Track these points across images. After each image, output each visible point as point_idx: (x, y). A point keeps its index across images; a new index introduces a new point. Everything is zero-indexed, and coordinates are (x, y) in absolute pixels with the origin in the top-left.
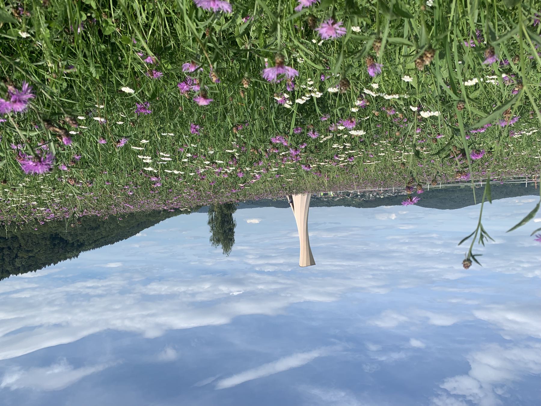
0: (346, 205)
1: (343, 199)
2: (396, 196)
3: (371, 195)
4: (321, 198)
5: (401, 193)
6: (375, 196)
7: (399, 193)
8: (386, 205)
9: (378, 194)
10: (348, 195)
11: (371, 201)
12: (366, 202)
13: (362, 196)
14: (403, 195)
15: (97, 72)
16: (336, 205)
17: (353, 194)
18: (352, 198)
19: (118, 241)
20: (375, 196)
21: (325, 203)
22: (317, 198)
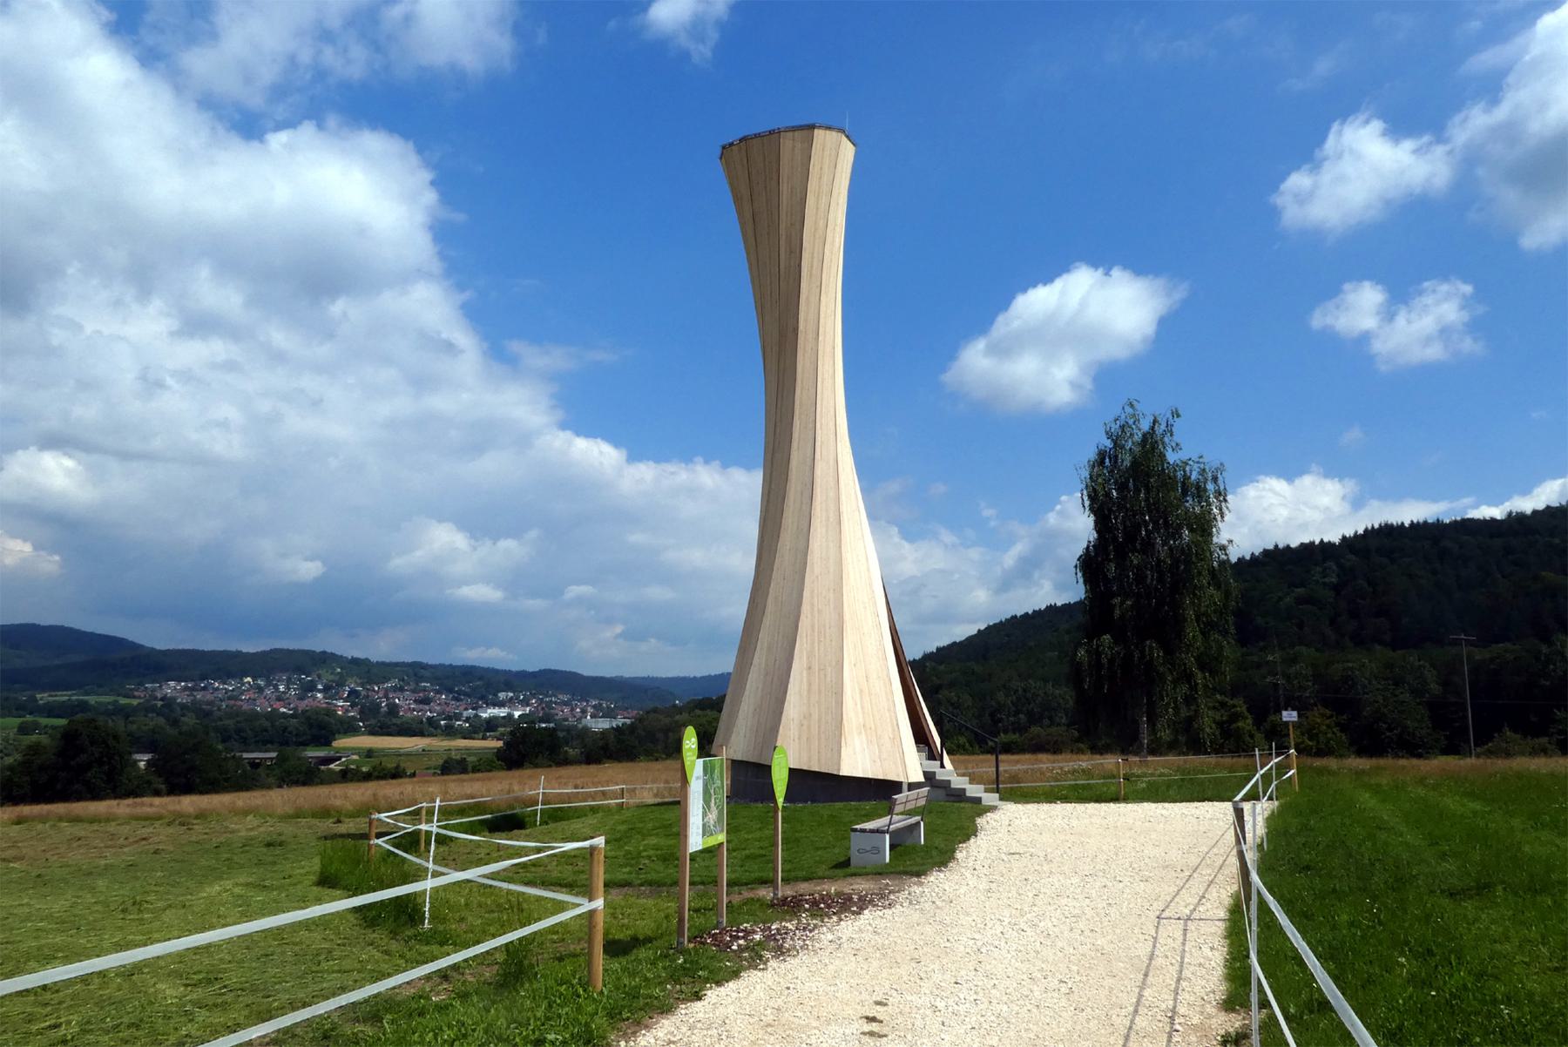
0: (366, 662)
1: (371, 682)
2: (202, 680)
3: (282, 688)
4: (438, 692)
5: (185, 689)
6: (269, 684)
7: (192, 689)
8: (238, 654)
9: (260, 690)
10: (353, 692)
11: (284, 670)
12: (300, 670)
13: (311, 687)
14: (179, 681)
15: (1011, 541)
16: (397, 664)
17: (338, 697)
18: (341, 684)
19: (1037, 613)
20: (269, 684)
21: (427, 674)
22: (450, 690)
